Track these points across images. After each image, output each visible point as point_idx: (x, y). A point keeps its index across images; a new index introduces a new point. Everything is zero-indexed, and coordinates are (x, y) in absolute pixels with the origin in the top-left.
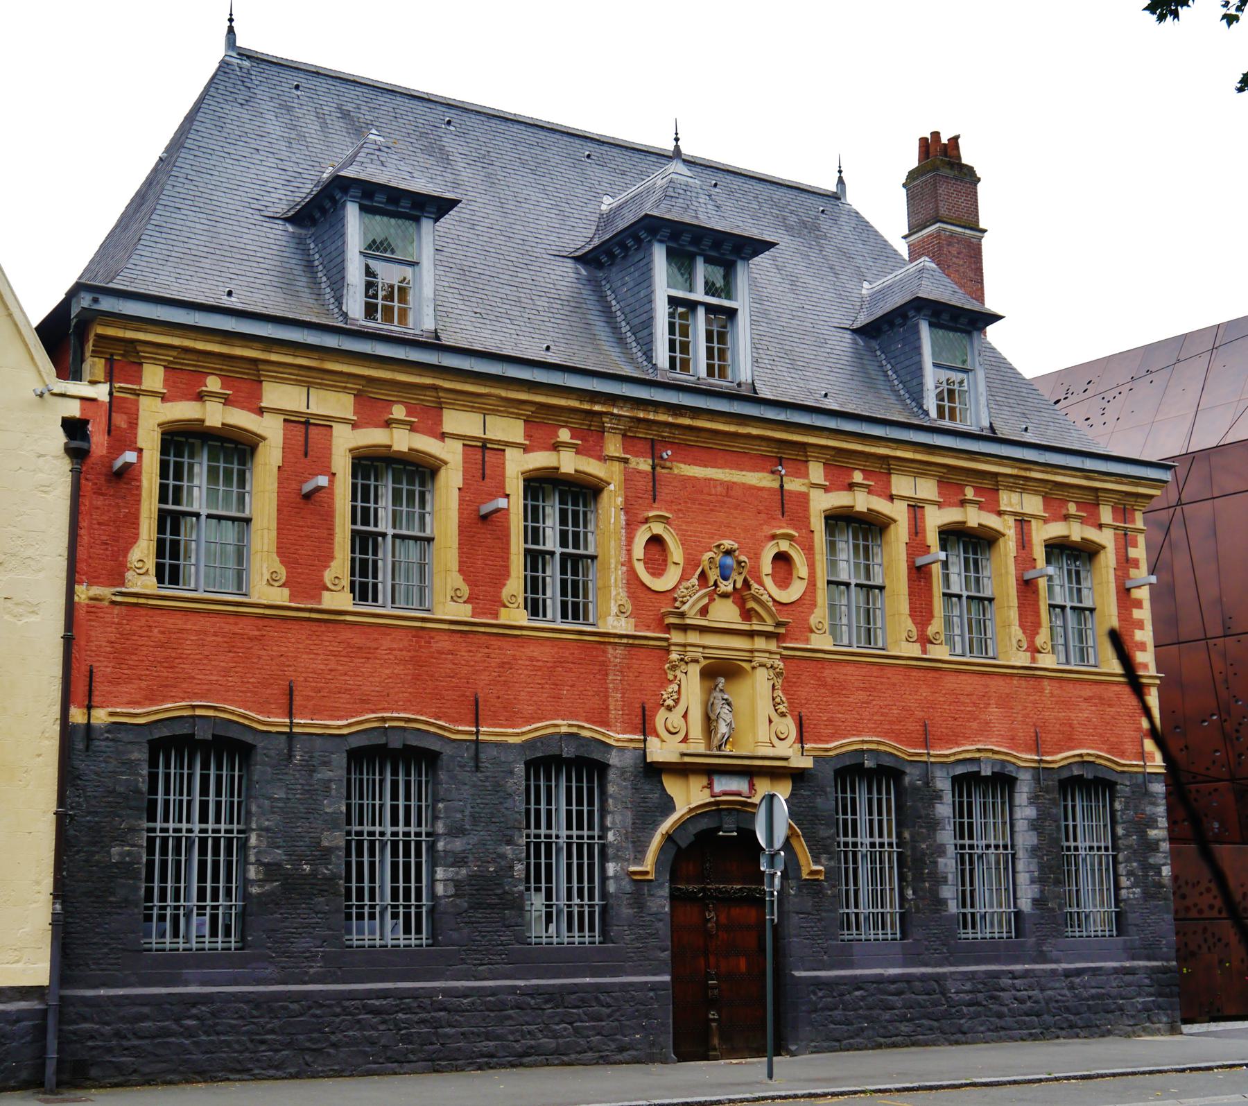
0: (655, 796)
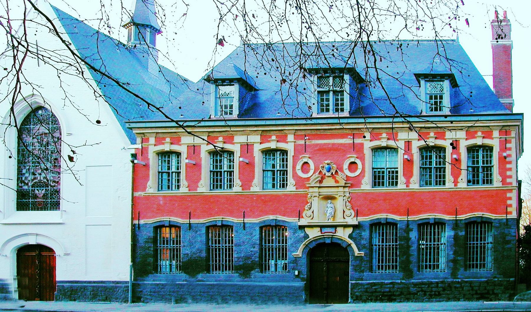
0: (303, 234)
